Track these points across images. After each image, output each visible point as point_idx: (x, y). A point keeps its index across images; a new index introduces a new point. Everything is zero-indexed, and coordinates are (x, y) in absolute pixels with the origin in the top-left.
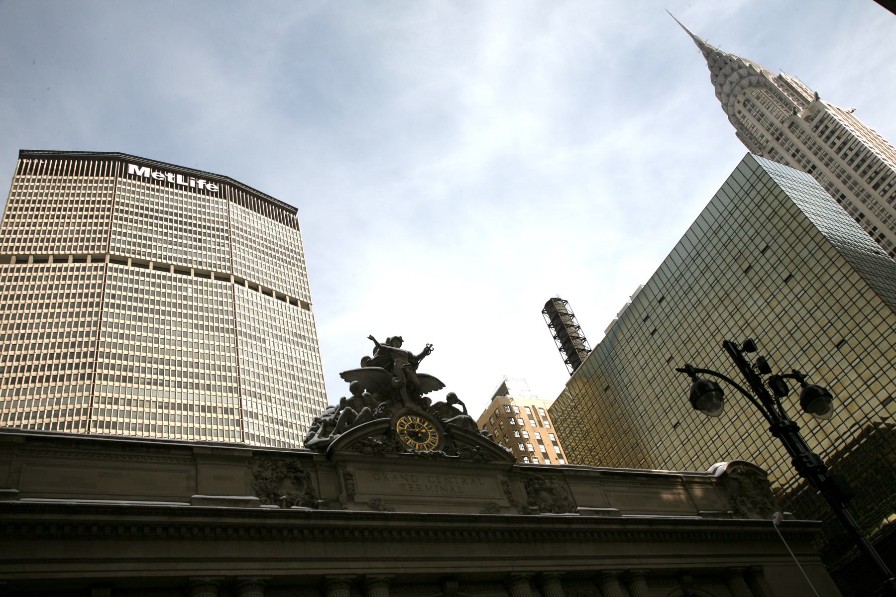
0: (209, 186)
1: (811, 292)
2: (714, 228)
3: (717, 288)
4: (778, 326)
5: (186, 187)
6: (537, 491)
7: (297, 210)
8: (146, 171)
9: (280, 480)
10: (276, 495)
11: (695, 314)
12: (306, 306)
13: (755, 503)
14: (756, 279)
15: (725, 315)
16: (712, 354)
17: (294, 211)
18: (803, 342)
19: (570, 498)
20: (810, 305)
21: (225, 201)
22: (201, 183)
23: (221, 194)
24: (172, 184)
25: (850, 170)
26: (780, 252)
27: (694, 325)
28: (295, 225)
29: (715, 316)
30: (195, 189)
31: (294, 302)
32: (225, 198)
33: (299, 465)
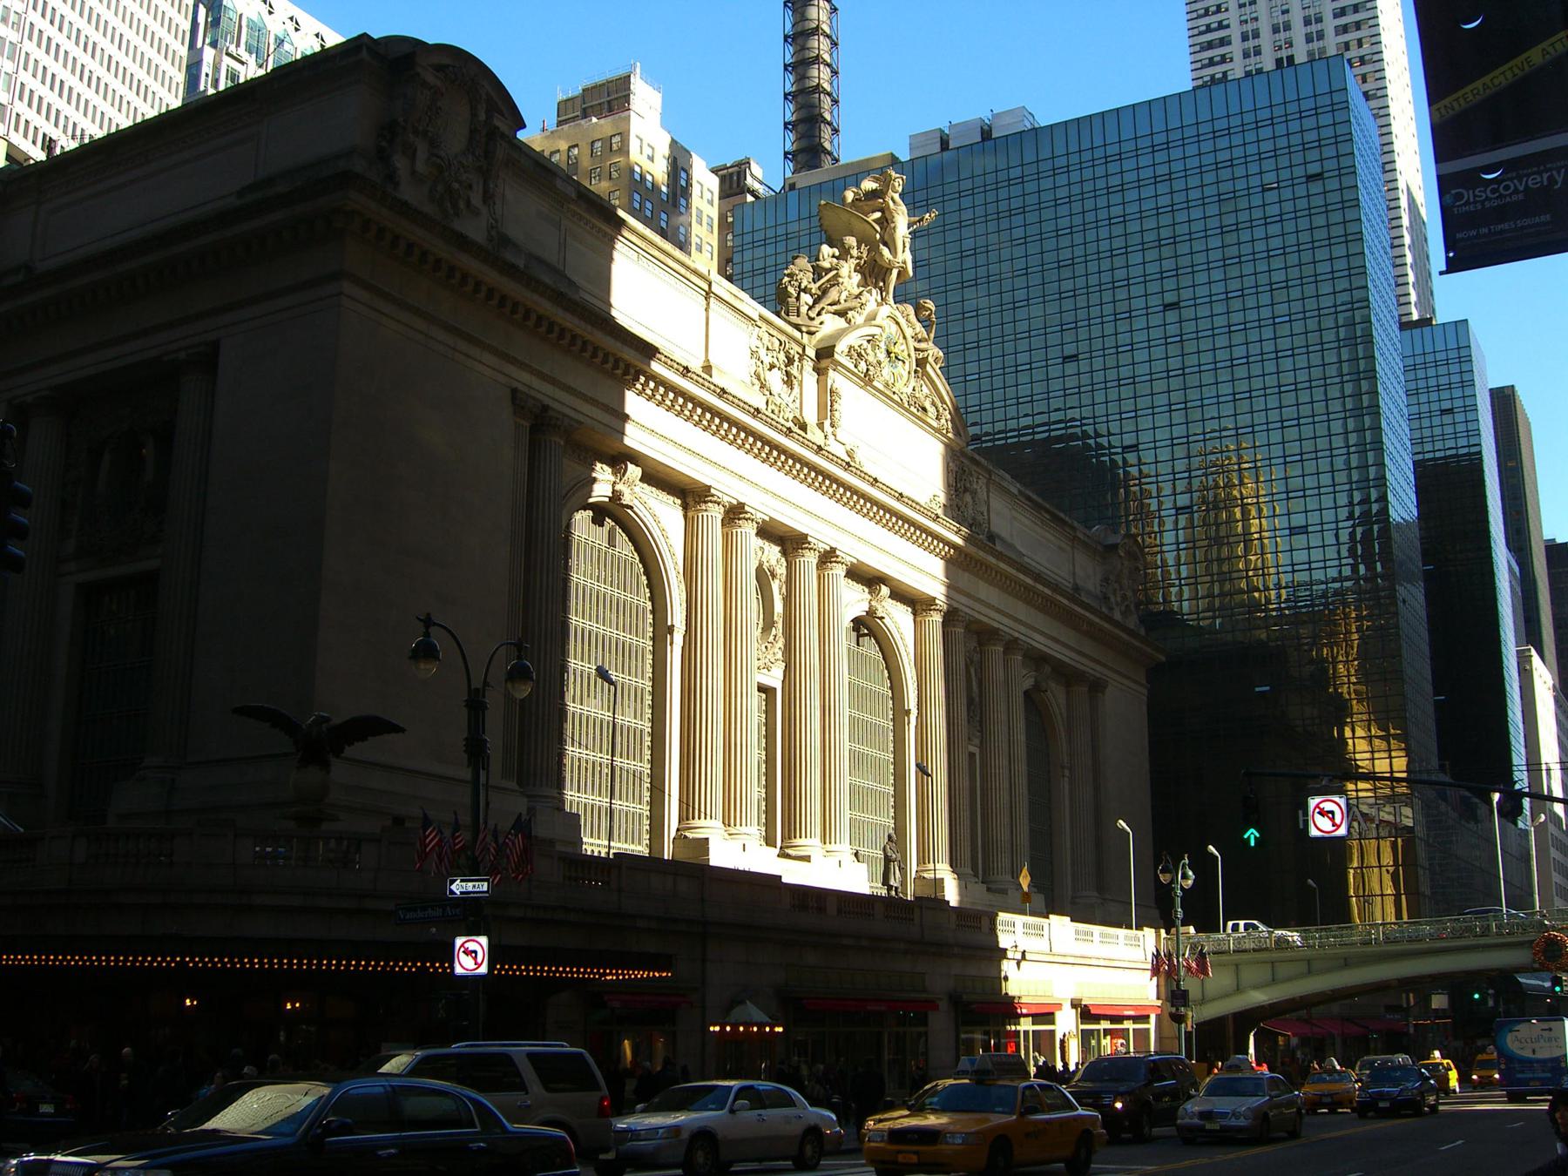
1: (1298, 327)
2: (1219, 125)
3: (1165, 220)
4: (1222, 341)
6: (966, 490)
9: (772, 367)
11: (1104, 233)
13: (1124, 597)
14: (1233, 251)
15: (1152, 268)
16: (1095, 311)
18: (1242, 386)
20: (1284, 343)
25: (1330, 24)
26: (1291, 240)
27: (1092, 248)
29: (1136, 258)
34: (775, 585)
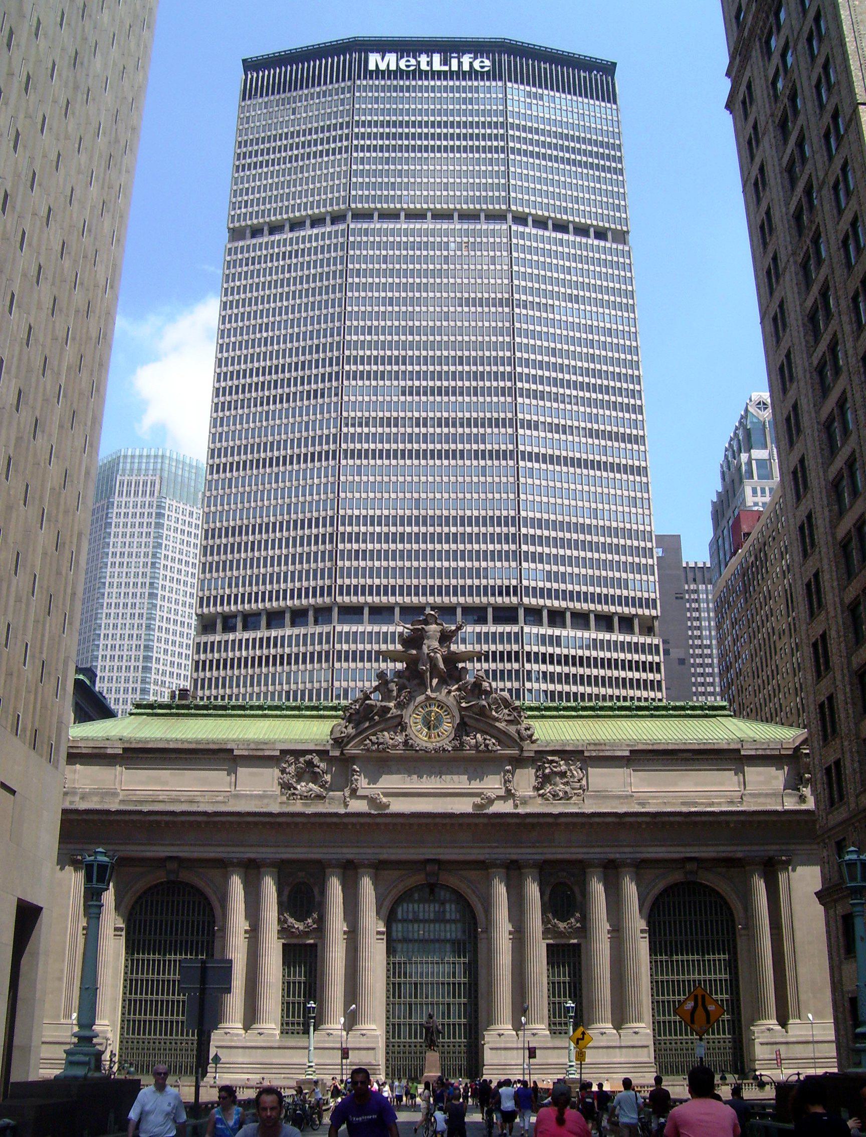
0: (477, 65)
5: (445, 72)
7: (614, 65)
8: (391, 59)
10: (295, 789)
12: (621, 237)
17: (609, 69)
19: (584, 782)
21: (500, 84)
22: (466, 59)
23: (493, 75)
24: (427, 72)
28: (610, 96)
30: (458, 72)
31: (601, 234)
32: (501, 79)
33: (316, 760)
34: (316, 891)
